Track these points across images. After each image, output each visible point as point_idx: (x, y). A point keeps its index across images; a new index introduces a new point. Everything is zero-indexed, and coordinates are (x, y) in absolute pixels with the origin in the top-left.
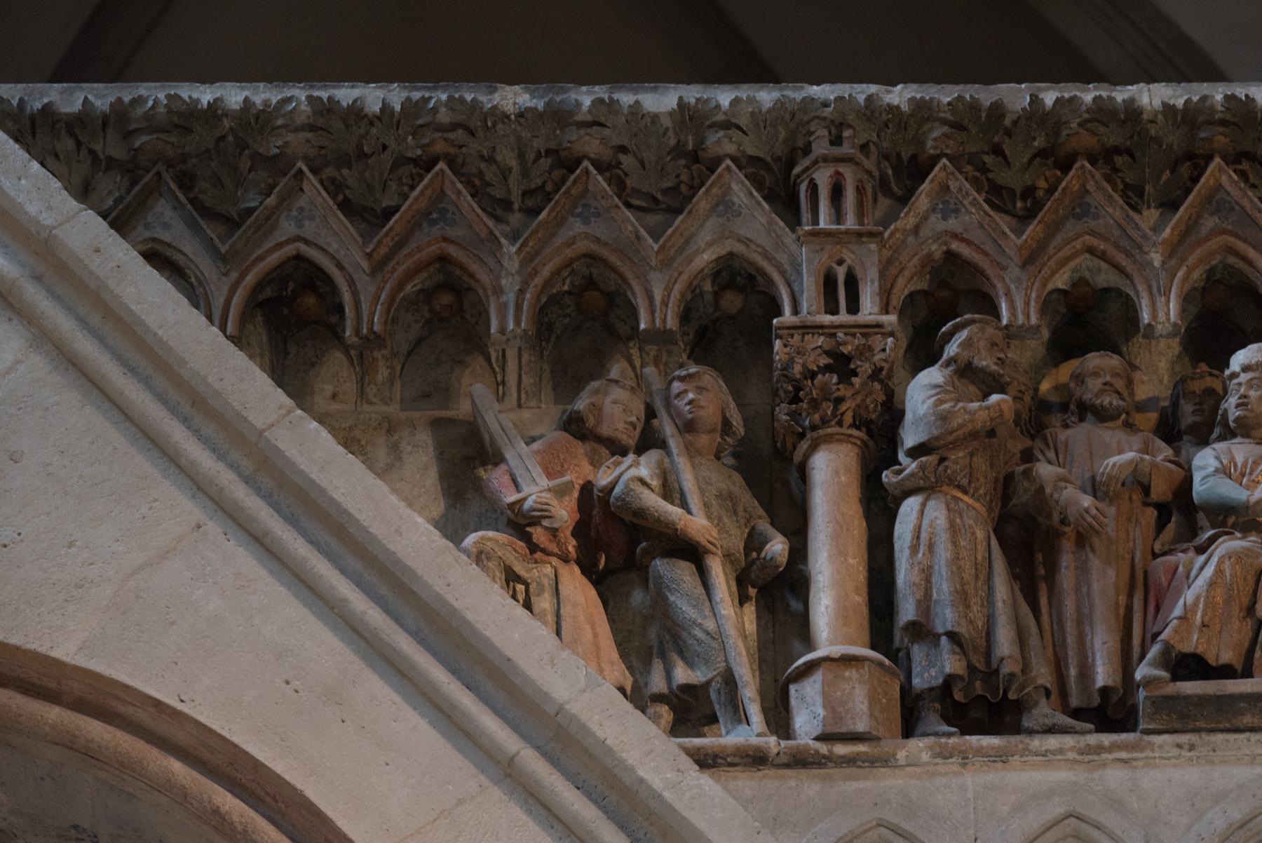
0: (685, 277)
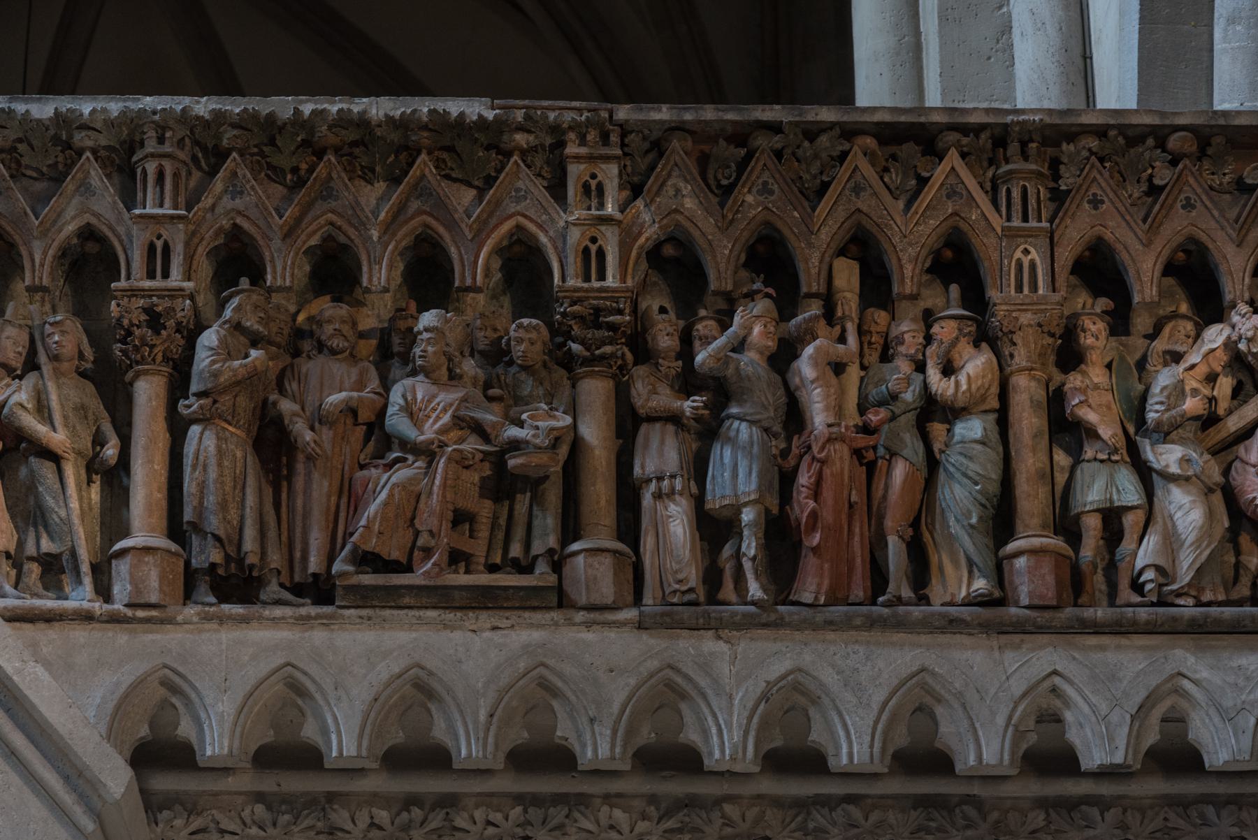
0: (56, 244)
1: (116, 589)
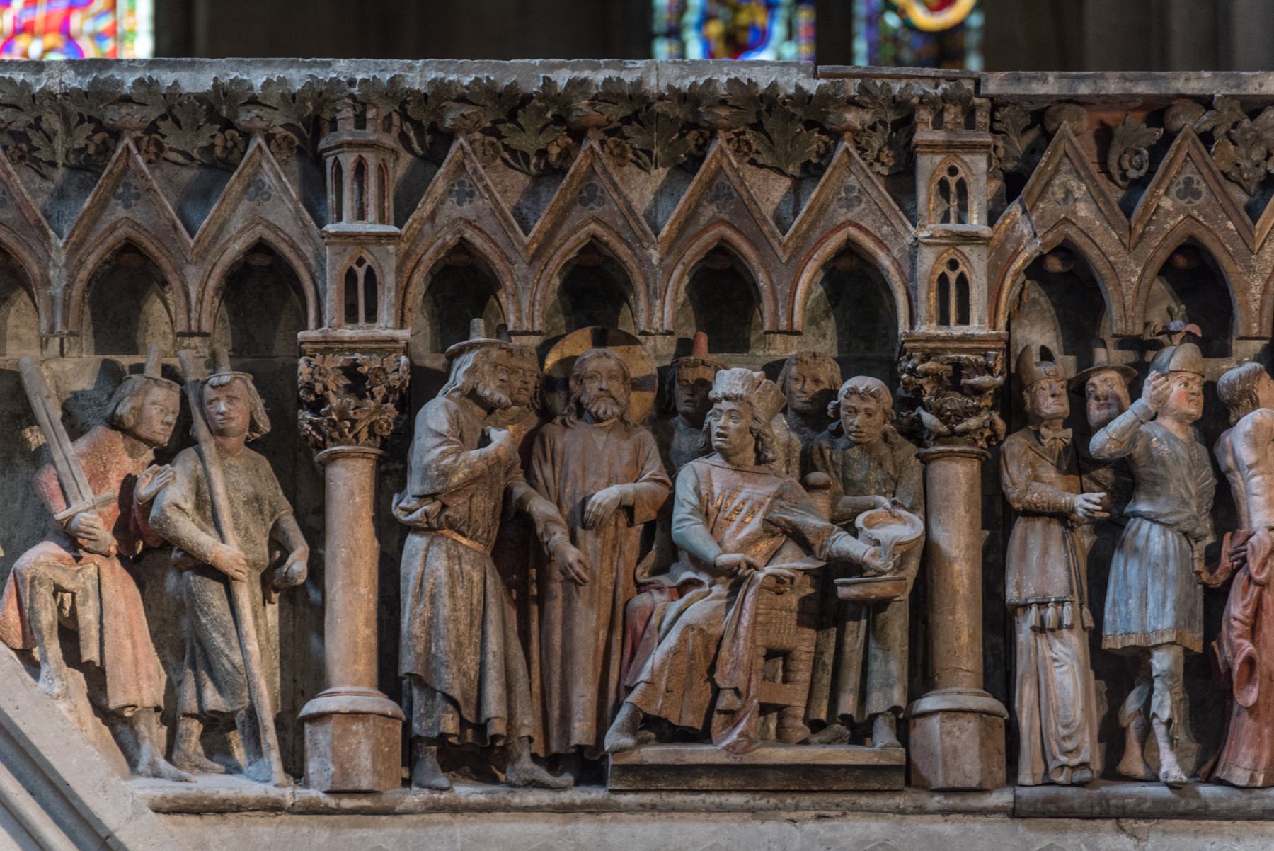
0: (218, 271)
1: (312, 766)
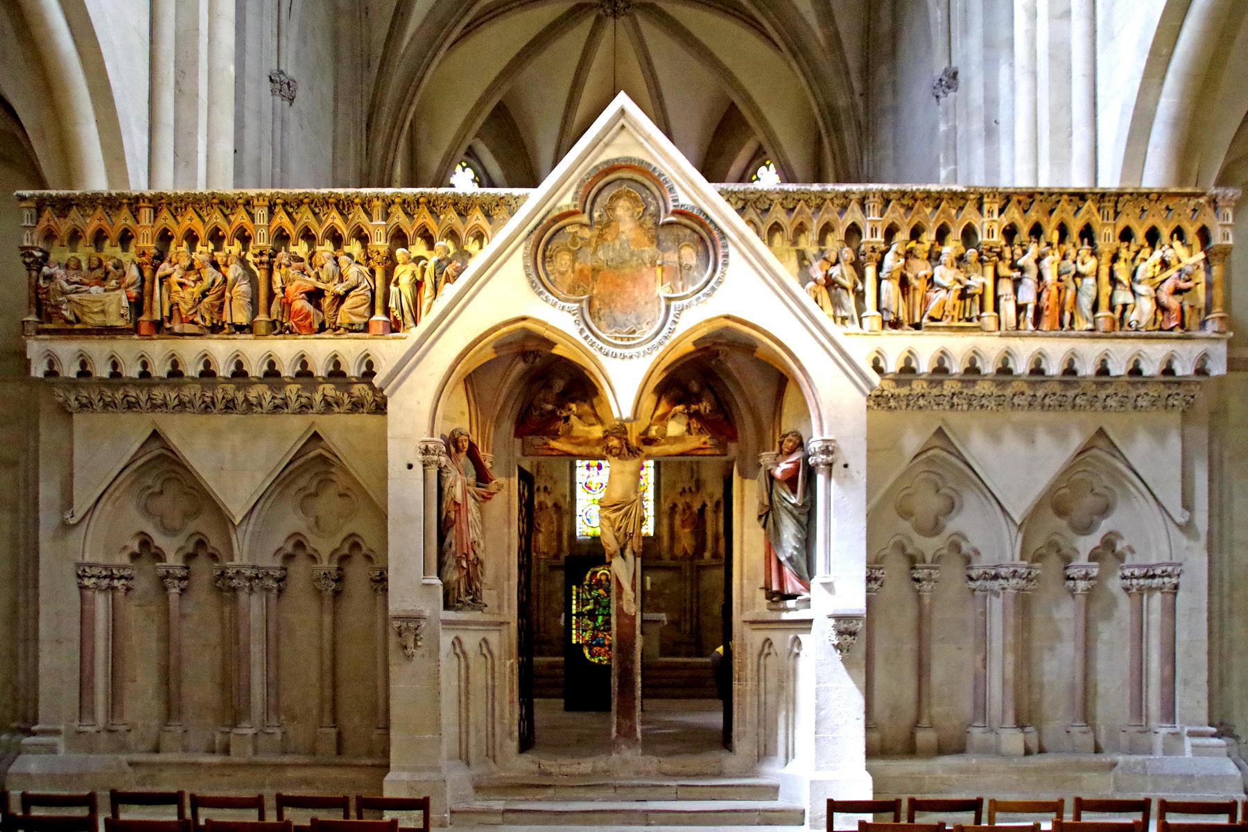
1: (864, 326)
